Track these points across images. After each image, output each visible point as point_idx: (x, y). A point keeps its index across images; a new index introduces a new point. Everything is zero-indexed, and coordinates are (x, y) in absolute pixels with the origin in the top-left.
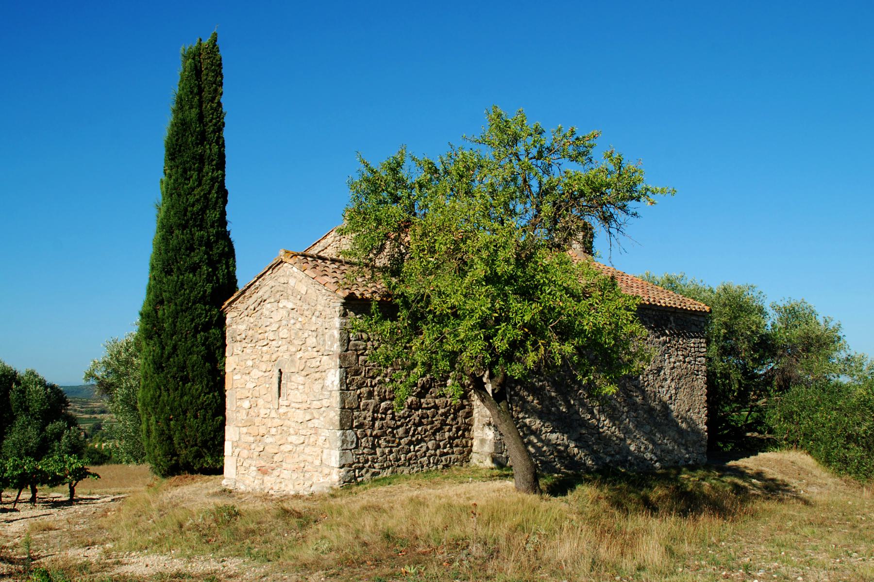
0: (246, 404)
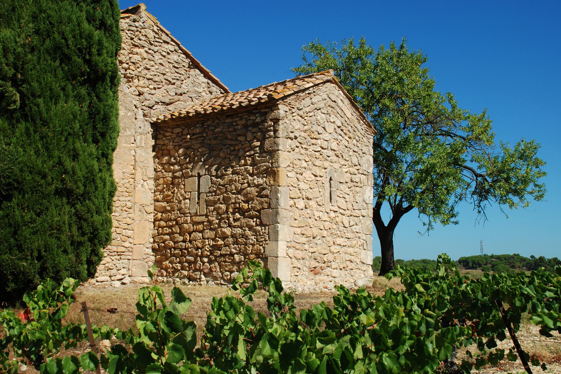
0: (301, 204)
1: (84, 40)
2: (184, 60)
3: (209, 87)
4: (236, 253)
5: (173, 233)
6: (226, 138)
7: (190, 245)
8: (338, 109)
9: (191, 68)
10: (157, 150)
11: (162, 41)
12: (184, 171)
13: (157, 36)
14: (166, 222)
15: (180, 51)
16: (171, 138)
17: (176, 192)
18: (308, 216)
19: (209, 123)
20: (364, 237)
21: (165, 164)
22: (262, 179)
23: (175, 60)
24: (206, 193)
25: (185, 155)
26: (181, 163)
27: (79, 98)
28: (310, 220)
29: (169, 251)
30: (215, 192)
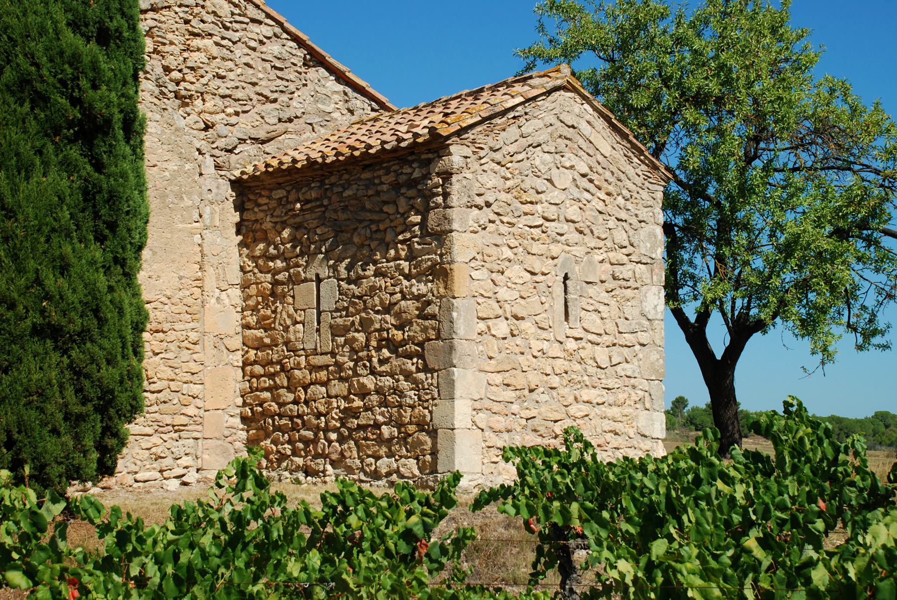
0: (502, 328)
1: (66, 66)
2: (294, 52)
3: (347, 101)
4: (385, 423)
5: (276, 387)
6: (363, 209)
7: (305, 408)
8: (581, 142)
9: (309, 67)
10: (244, 231)
11: (247, 20)
12: (292, 271)
13: (237, 11)
14: (263, 366)
15: (285, 36)
16: (269, 209)
17: (279, 310)
18: (517, 350)
19: (333, 179)
20: (645, 385)
21: (259, 257)
22: (425, 285)
23: (276, 54)
24: (331, 312)
25: (294, 240)
26: (287, 255)
27: (68, 166)
28: (521, 358)
29: (270, 421)
30: (346, 309)
